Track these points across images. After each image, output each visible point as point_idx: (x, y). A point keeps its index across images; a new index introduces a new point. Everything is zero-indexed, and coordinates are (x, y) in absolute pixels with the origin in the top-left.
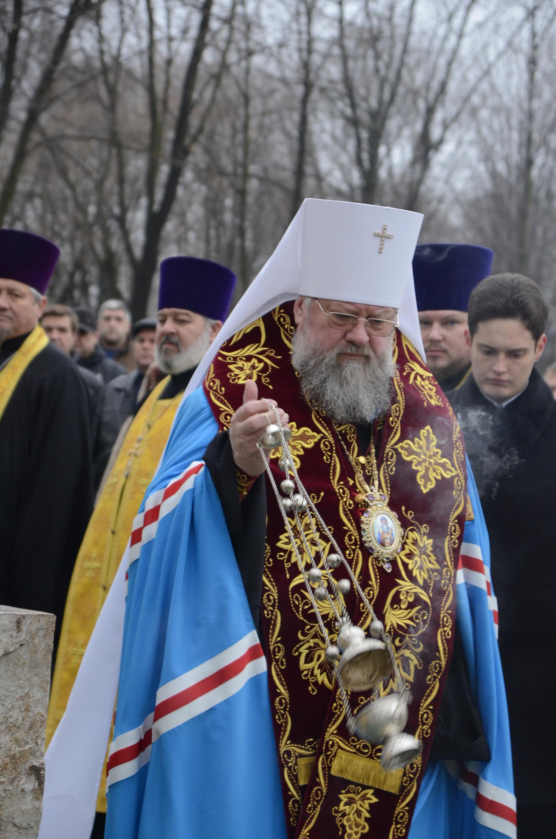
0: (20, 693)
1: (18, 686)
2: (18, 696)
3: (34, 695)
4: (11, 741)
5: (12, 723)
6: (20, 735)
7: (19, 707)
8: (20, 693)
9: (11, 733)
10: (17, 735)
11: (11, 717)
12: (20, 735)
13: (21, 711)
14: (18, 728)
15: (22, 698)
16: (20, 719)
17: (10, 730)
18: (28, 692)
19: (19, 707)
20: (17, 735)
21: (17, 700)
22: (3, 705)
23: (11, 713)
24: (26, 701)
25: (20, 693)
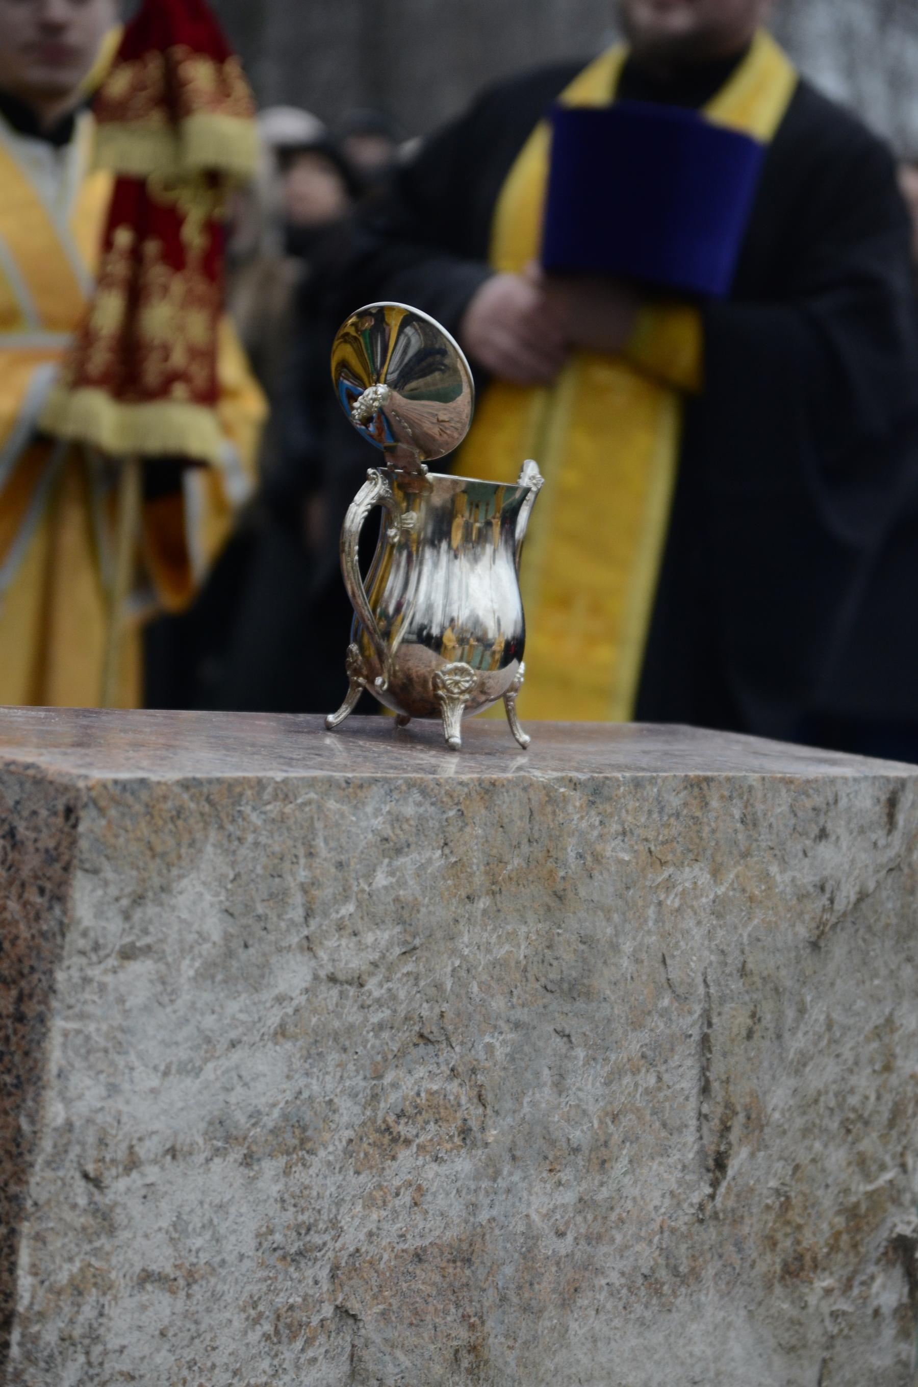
0: (874, 1017)
1: (872, 996)
2: (869, 1028)
3: (904, 1022)
4: (849, 1164)
5: (854, 1110)
6: (869, 1144)
7: (871, 1061)
8: (874, 1017)
9: (850, 1139)
10: (865, 1145)
11: (852, 1091)
12: (869, 1144)
13: (874, 1071)
14: (866, 1123)
15: (877, 1033)
16: (873, 1097)
17: (849, 1131)
18: (891, 1014)
19: (871, 1061)
20: (865, 1145)
21: (868, 1040)
22: (838, 1056)
23: (853, 1080)
24: (886, 1040)
25: (876, 1017)
